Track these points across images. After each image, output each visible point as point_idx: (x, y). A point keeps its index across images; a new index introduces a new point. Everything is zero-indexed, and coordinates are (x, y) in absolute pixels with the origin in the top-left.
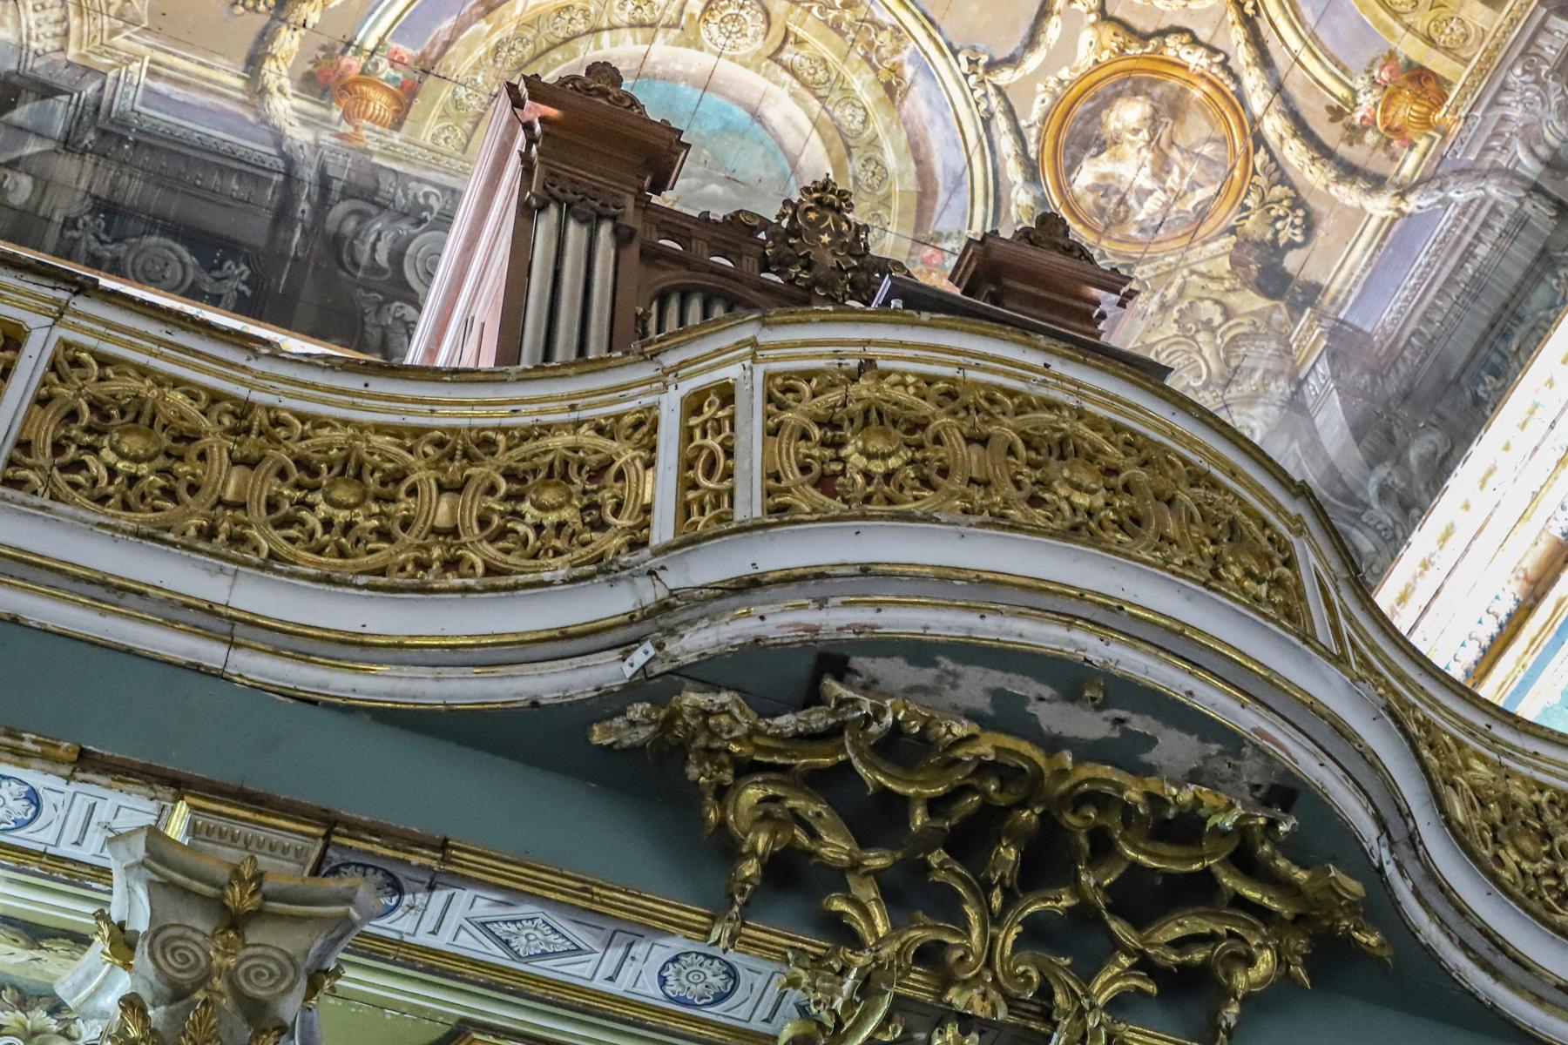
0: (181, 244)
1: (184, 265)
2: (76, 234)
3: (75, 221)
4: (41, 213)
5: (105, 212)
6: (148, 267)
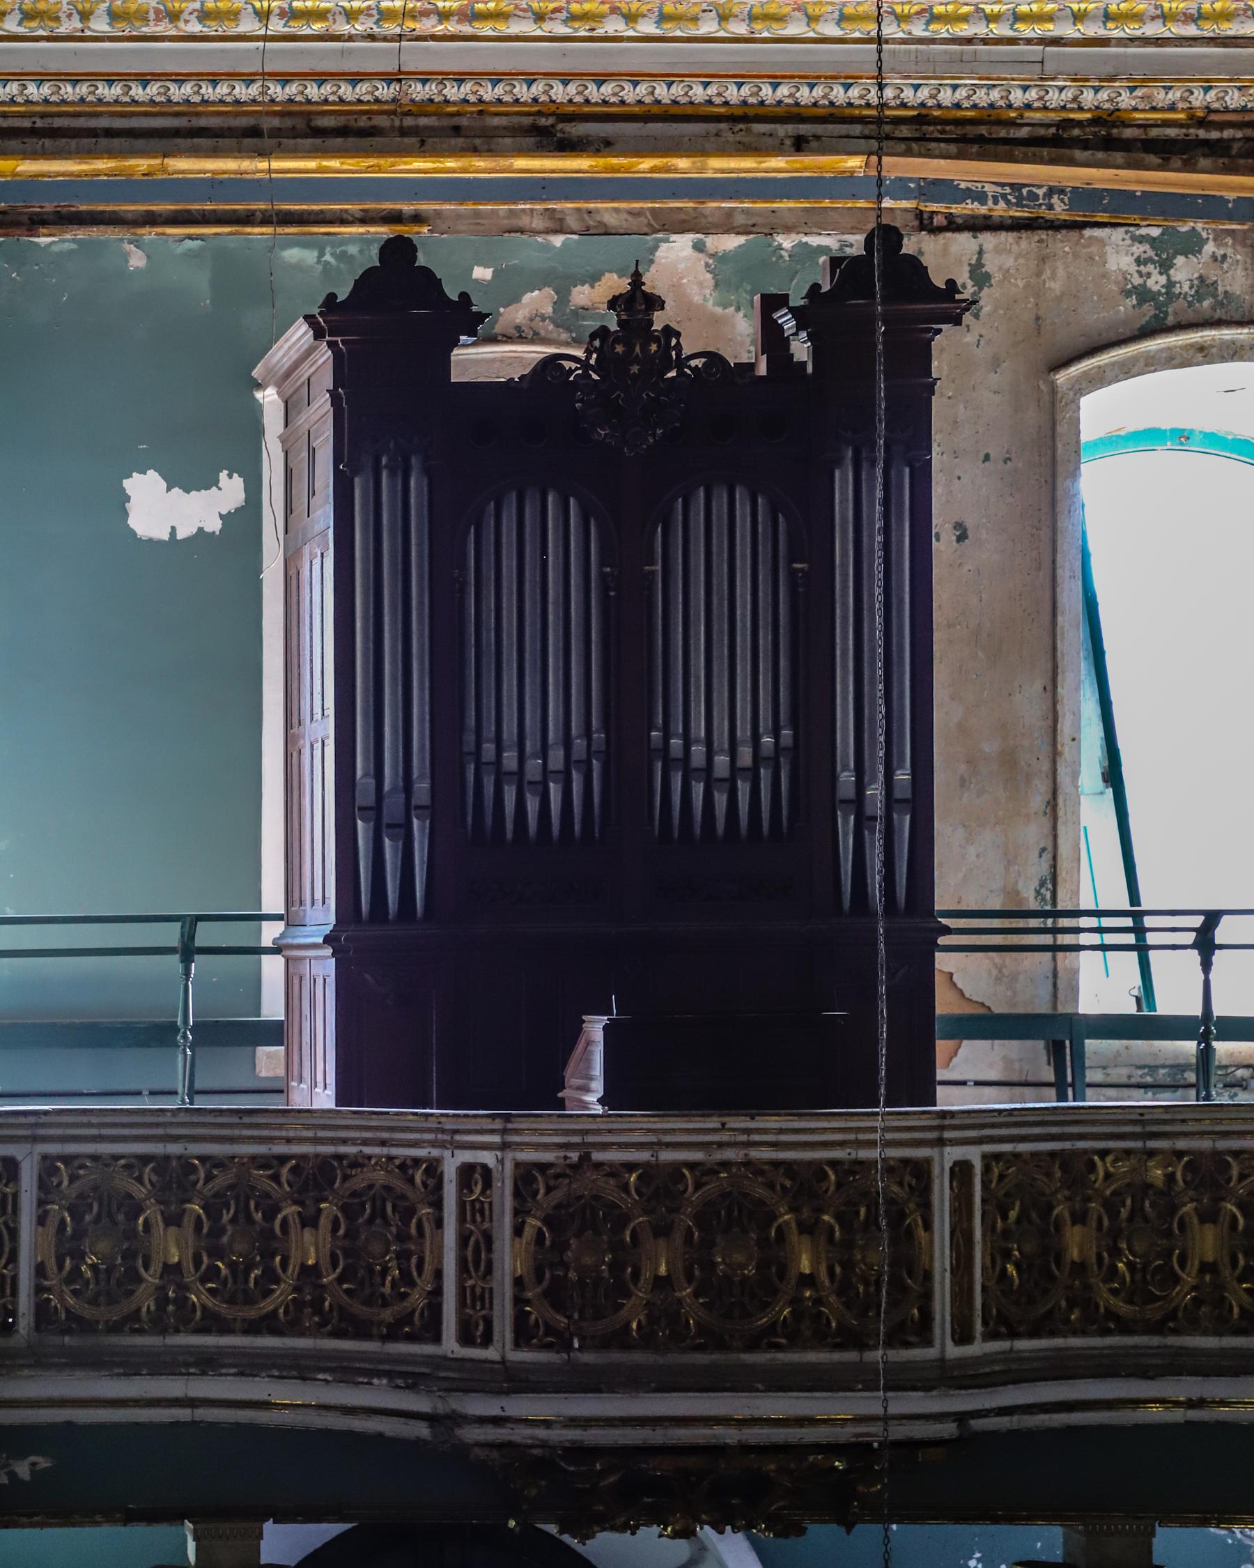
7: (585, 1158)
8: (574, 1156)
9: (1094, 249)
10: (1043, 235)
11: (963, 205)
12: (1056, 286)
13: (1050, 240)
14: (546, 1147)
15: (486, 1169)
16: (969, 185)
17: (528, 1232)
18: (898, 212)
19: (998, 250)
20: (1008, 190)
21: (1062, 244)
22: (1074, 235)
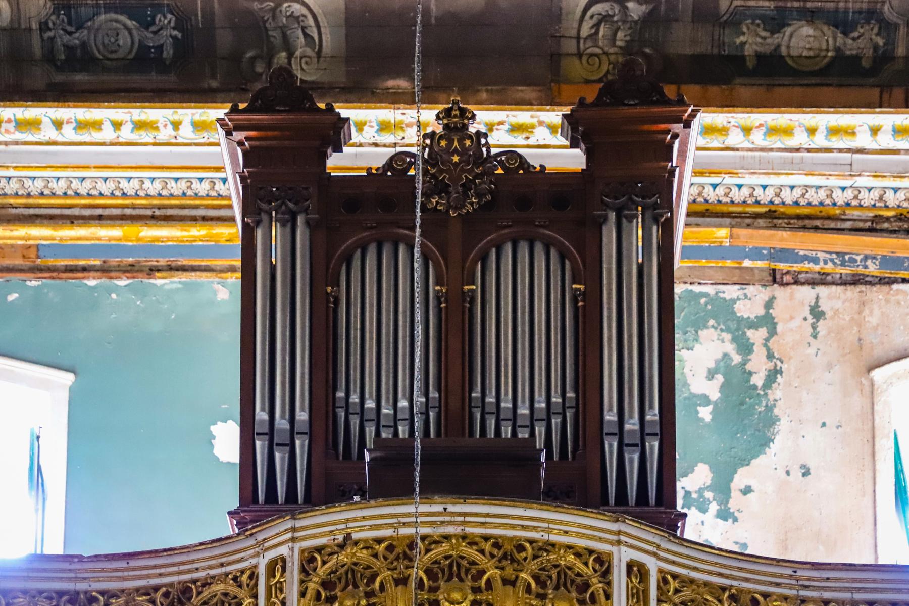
0: (121, 14)
1: (129, 31)
2: (51, 34)
3: (46, 23)
4: (23, 27)
5: (63, 8)
6: (106, 42)
7: (348, 537)
8: (340, 538)
9: (900, 297)
10: (862, 288)
11: (802, 265)
12: (874, 320)
13: (868, 292)
14: (322, 535)
15: (284, 560)
16: (807, 253)
17: (310, 594)
18: (756, 271)
19: (830, 298)
20: (834, 256)
21: (877, 294)
22: (885, 288)
